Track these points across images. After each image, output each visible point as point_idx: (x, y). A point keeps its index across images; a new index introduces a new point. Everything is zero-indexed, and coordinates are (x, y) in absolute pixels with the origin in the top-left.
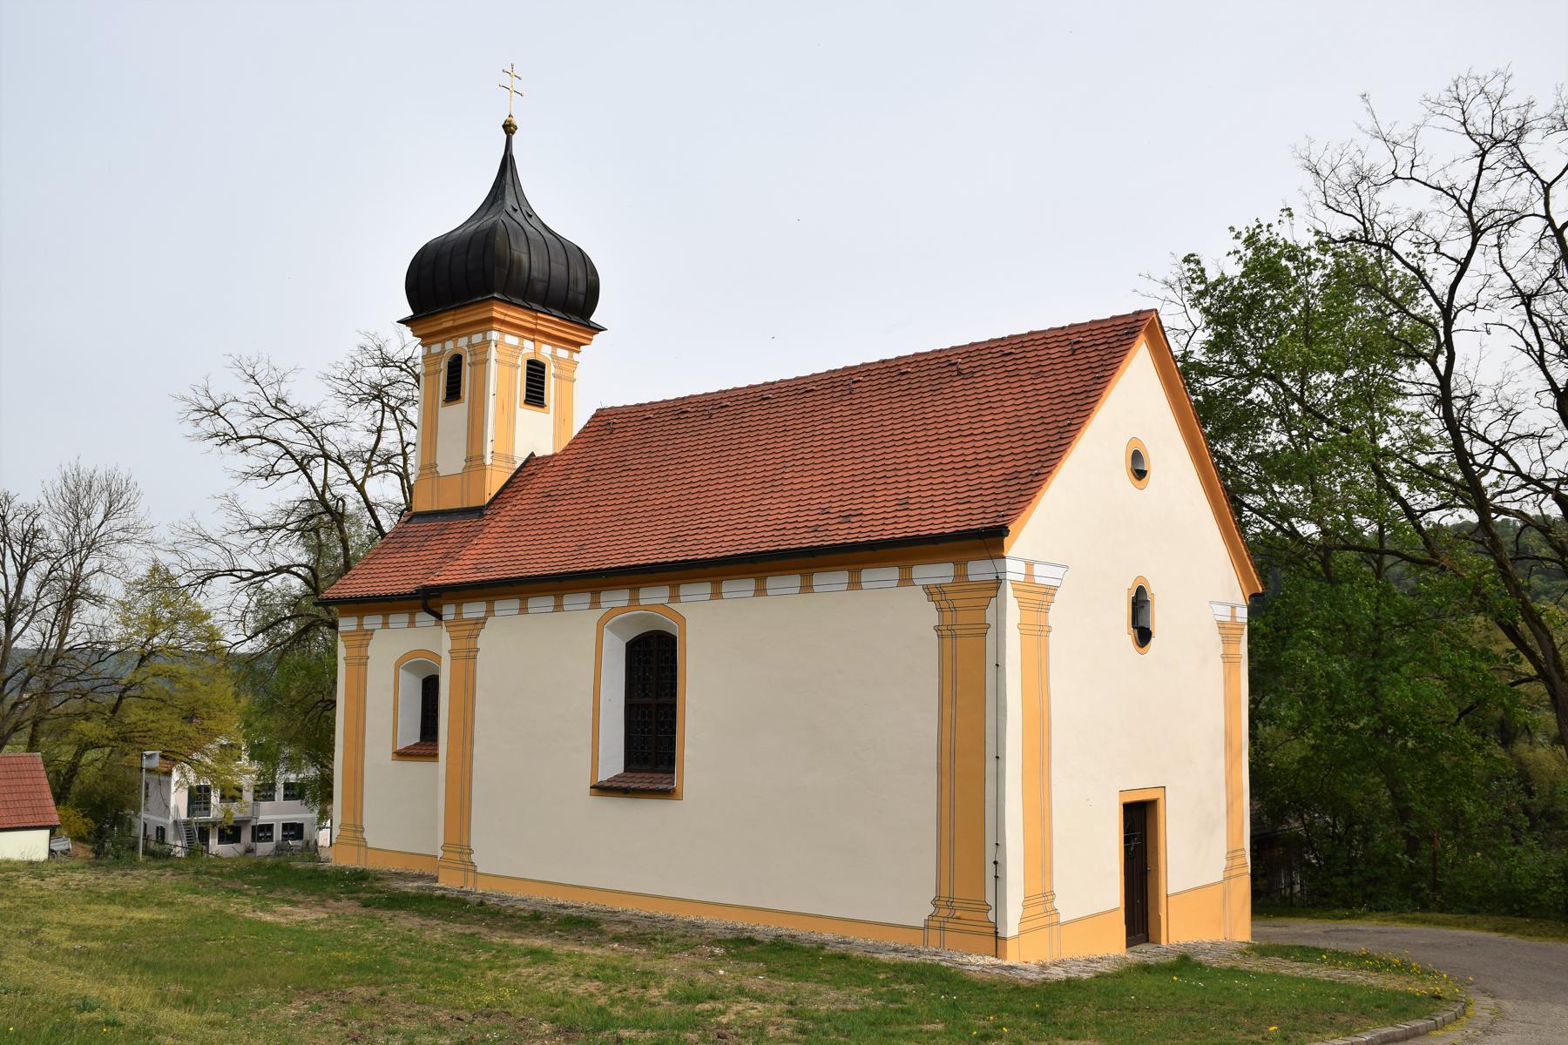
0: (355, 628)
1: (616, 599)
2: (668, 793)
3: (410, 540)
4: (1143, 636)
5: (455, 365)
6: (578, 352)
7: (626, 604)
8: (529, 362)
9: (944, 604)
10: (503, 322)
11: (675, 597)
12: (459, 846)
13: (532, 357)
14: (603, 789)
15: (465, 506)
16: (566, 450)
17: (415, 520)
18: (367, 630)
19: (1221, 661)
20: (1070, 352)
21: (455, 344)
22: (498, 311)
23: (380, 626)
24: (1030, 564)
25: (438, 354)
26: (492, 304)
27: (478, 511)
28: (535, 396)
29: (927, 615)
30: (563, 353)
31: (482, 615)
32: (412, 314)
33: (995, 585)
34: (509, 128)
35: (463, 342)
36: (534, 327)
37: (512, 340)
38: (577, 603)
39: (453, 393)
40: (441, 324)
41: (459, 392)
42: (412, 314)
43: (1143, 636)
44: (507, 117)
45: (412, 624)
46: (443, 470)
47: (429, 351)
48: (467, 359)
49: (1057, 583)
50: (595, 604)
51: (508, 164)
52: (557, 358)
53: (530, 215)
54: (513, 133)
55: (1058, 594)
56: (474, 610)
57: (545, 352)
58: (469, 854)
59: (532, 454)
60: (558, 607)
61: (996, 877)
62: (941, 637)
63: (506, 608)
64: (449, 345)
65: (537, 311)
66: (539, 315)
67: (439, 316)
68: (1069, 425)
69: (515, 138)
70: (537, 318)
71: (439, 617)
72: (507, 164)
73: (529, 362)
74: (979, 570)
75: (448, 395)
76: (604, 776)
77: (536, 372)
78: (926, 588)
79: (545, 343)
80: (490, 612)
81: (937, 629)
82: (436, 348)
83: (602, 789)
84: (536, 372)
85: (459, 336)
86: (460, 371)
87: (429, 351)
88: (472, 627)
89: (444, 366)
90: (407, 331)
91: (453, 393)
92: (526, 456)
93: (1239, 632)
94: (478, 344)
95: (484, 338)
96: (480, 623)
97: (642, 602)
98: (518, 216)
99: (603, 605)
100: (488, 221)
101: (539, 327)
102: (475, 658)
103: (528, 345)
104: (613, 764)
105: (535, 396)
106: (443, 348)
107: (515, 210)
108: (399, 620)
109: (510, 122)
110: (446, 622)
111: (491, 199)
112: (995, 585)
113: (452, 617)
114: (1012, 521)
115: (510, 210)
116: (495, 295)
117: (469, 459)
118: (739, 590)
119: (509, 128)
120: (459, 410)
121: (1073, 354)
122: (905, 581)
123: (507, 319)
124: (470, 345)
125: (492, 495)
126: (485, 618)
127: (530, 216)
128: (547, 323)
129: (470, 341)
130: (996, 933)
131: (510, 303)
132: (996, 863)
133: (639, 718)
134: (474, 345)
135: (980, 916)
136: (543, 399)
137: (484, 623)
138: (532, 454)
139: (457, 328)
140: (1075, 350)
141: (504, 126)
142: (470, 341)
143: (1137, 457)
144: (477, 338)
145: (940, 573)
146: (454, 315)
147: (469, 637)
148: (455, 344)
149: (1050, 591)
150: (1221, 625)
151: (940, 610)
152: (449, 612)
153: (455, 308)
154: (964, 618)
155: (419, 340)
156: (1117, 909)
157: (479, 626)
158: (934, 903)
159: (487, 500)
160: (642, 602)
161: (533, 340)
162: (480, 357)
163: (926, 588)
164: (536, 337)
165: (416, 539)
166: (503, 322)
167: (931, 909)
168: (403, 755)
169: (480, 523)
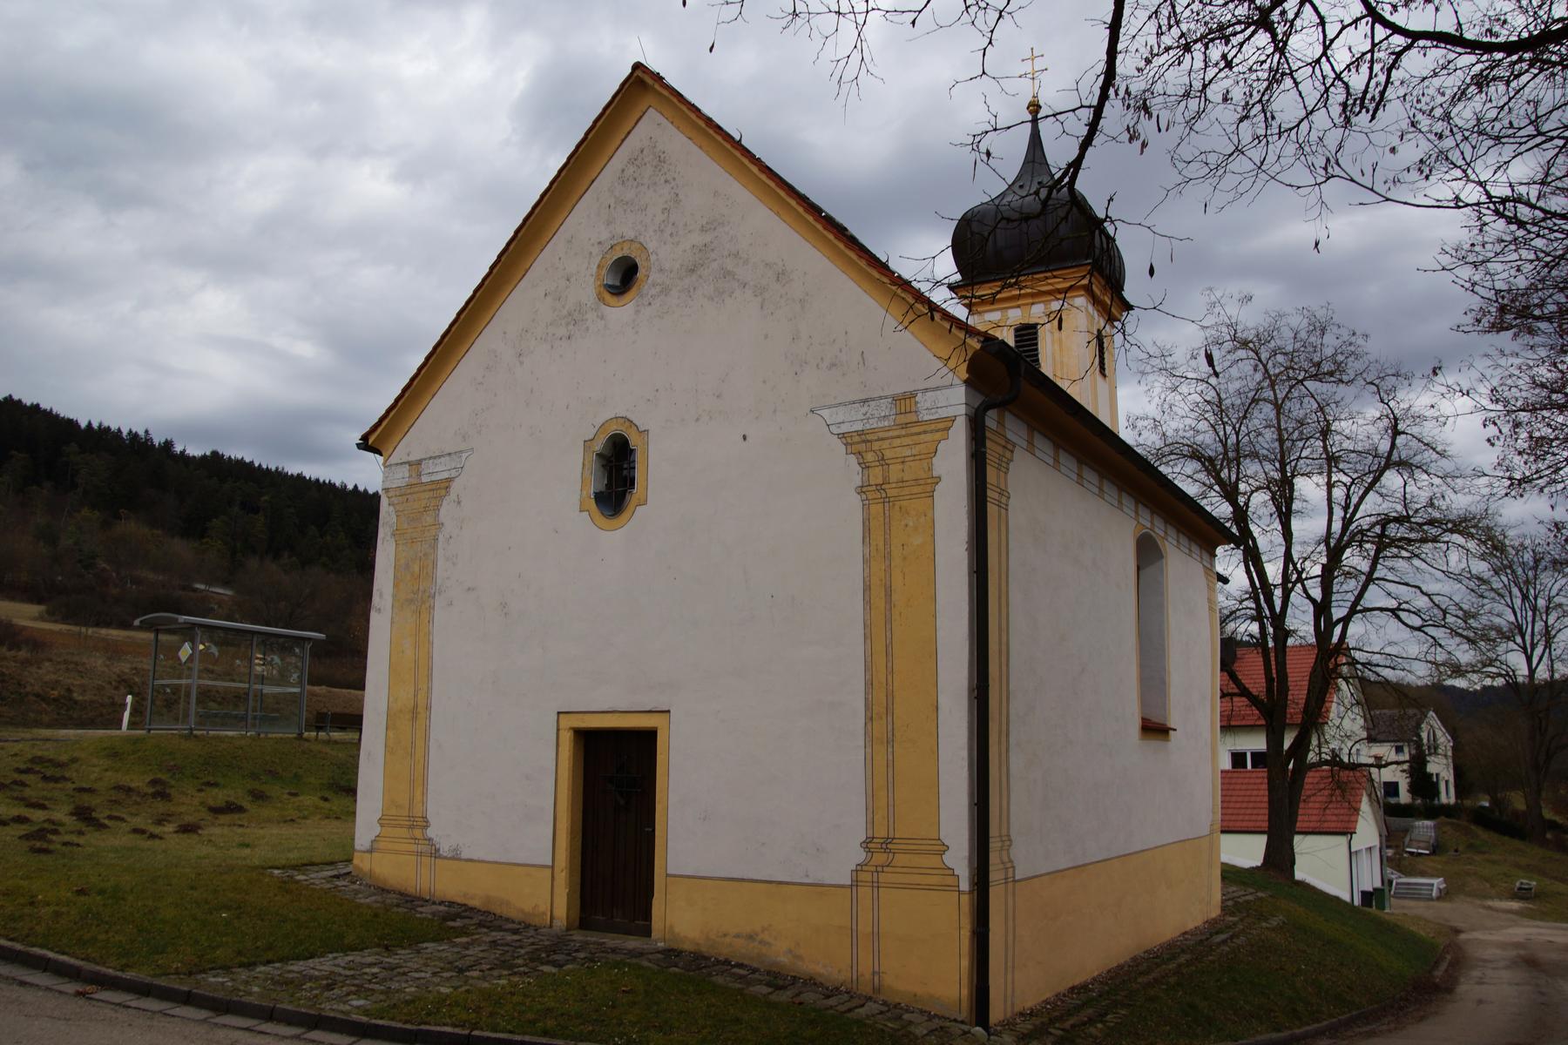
19: (856, 500)
49: (454, 474)
55: (456, 487)
150: (858, 443)
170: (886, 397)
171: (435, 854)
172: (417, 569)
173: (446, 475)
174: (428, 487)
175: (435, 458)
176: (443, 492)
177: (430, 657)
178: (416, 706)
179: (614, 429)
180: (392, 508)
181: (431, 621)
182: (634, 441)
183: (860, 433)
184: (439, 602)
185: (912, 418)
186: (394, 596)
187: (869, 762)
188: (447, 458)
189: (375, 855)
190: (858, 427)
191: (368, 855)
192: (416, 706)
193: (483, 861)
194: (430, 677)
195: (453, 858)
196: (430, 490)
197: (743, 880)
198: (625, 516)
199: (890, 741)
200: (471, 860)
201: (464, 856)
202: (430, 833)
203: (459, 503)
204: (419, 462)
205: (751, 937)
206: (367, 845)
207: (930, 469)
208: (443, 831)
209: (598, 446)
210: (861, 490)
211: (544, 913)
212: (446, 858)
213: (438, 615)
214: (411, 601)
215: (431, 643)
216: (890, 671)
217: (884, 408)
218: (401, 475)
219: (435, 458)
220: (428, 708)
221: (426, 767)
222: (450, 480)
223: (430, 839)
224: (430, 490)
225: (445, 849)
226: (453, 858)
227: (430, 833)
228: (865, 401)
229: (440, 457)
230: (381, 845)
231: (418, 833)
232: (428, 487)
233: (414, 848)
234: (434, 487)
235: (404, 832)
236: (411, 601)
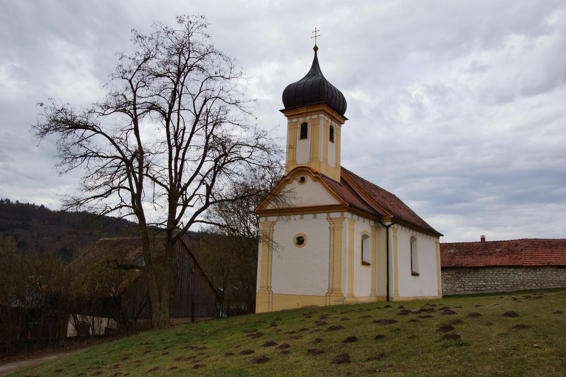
30: (337, 126)
34: (316, 49)
35: (308, 118)
37: (326, 118)
39: (304, 135)
40: (299, 111)
41: (307, 135)
64: (301, 120)
69: (317, 52)
72: (316, 62)
75: (301, 136)
82: (295, 120)
85: (307, 116)
87: (291, 121)
90: (282, 115)
91: (304, 135)
119: (316, 49)
129: (311, 117)
134: (313, 119)
139: (306, 113)
142: (311, 117)
144: (314, 117)
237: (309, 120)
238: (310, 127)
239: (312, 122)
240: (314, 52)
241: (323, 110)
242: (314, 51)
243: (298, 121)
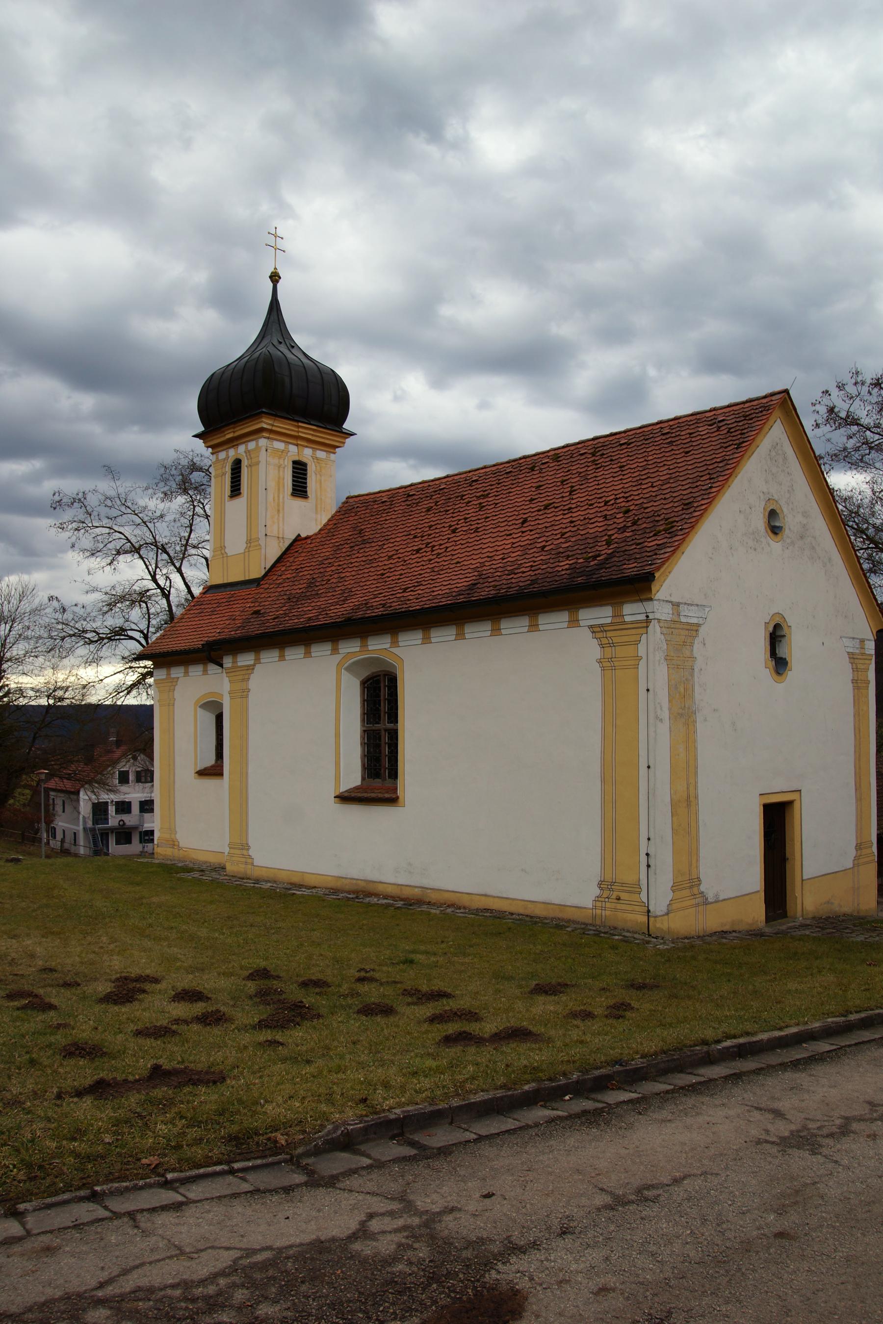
0: (164, 677)
1: (350, 648)
2: (392, 800)
3: (207, 606)
4: (780, 664)
5: (237, 467)
6: (335, 453)
7: (358, 649)
8: (294, 462)
9: (605, 641)
10: (270, 431)
11: (395, 643)
12: (242, 846)
13: (296, 458)
14: (345, 798)
15: (247, 579)
16: (321, 530)
17: (210, 592)
18: (174, 678)
19: (851, 685)
20: (716, 429)
21: (236, 452)
22: (266, 423)
23: (182, 675)
24: (676, 605)
25: (224, 459)
26: (262, 417)
27: (256, 582)
28: (300, 489)
29: (592, 649)
30: (321, 454)
31: (252, 662)
32: (203, 429)
33: (645, 625)
35: (242, 449)
36: (296, 434)
37: (279, 445)
38: (321, 651)
39: (236, 490)
40: (225, 435)
41: (239, 489)
42: (203, 429)
43: (780, 664)
44: (273, 270)
45: (186, 673)
46: (230, 551)
47: (217, 458)
48: (245, 463)
49: (701, 621)
50: (335, 651)
51: (275, 306)
52: (317, 459)
53: (293, 346)
54: (277, 281)
55: (702, 630)
56: (245, 659)
57: (307, 454)
58: (248, 850)
59: (299, 535)
60: (308, 654)
61: (648, 866)
62: (603, 669)
63: (269, 657)
64: (232, 453)
65: (298, 421)
66: (300, 424)
67: (222, 430)
68: (711, 487)
69: (279, 286)
70: (299, 427)
71: (221, 665)
73: (294, 462)
74: (632, 611)
75: (232, 491)
76: (343, 788)
77: (300, 470)
78: (591, 627)
79: (307, 447)
80: (258, 660)
81: (600, 662)
82: (222, 455)
83: (345, 798)
84: (300, 470)
85: (237, 445)
86: (240, 472)
88: (244, 672)
89: (228, 469)
90: (200, 442)
91: (236, 490)
92: (294, 538)
93: (867, 662)
94: (253, 450)
95: (257, 445)
96: (251, 668)
97: (370, 648)
98: (282, 348)
99: (341, 651)
100: (262, 350)
101: (301, 434)
102: (247, 696)
103: (293, 449)
104: (353, 777)
105: (300, 489)
106: (227, 455)
107: (281, 343)
108: (196, 671)
109: (276, 272)
110: (227, 669)
111: (263, 334)
112: (645, 625)
113: (230, 665)
114: (658, 569)
115: (276, 343)
116: (264, 410)
117: (249, 541)
118: (443, 636)
120: (240, 503)
121: (718, 430)
122: (574, 622)
123: (274, 428)
124: (247, 452)
125: (268, 567)
126: (254, 665)
127: (293, 347)
128: (306, 431)
129: (247, 448)
130: (649, 911)
131: (276, 416)
132: (647, 854)
133: (372, 741)
134: (249, 451)
135: (635, 897)
136: (306, 492)
137: (253, 669)
138: (299, 535)
140: (719, 427)
141: (271, 277)
142: (247, 448)
143: (772, 514)
144: (252, 445)
145: (602, 615)
146: (234, 428)
147: (243, 680)
148: (236, 452)
149: (694, 629)
150: (852, 656)
151: (602, 646)
152: (228, 661)
153: (234, 423)
154: (620, 651)
155: (210, 450)
156: (758, 891)
157: (250, 671)
158: (600, 885)
159: (263, 572)
160: (370, 648)
161: (297, 445)
162: (254, 460)
163: (591, 627)
164: (299, 442)
165: (210, 606)
166: (270, 431)
167: (598, 892)
168: (203, 773)
169: (256, 591)
170: (857, 639)
171: (706, 903)
172: (682, 690)
173: (695, 621)
174: (685, 627)
175: (688, 604)
176: (694, 633)
177: (696, 759)
178: (688, 797)
179: (777, 620)
180: (663, 637)
181: (695, 732)
182: (786, 631)
183: (853, 654)
184: (699, 718)
185: (863, 651)
186: (670, 709)
187: (857, 808)
188: (696, 608)
189: (671, 915)
190: (851, 650)
191: (666, 917)
192: (688, 797)
193: (730, 898)
194: (696, 773)
195: (716, 902)
196: (687, 630)
197: (826, 875)
198: (784, 676)
199: (861, 800)
200: (724, 900)
201: (721, 898)
202: (702, 888)
203: (704, 644)
204: (678, 605)
205: (828, 902)
206: (665, 910)
207: (867, 677)
208: (709, 887)
209: (771, 629)
210: (853, 681)
211: (757, 921)
212: (712, 903)
213: (698, 725)
214: (681, 715)
215: (696, 748)
216: (860, 768)
217: (857, 643)
218: (666, 611)
219: (688, 604)
220: (696, 797)
221: (698, 841)
222: (698, 625)
223: (702, 893)
224: (687, 630)
225: (711, 898)
226: (716, 902)
227: (702, 888)
228: (854, 638)
229: (692, 605)
230: (674, 906)
231: (695, 890)
232: (685, 627)
233: (694, 902)
234: (688, 627)
235: (686, 893)
236: (681, 715)
237: (244, 454)
238: (246, 468)
239: (248, 459)
240: (271, 285)
241: (262, 430)
242: (272, 281)
243: (228, 457)
